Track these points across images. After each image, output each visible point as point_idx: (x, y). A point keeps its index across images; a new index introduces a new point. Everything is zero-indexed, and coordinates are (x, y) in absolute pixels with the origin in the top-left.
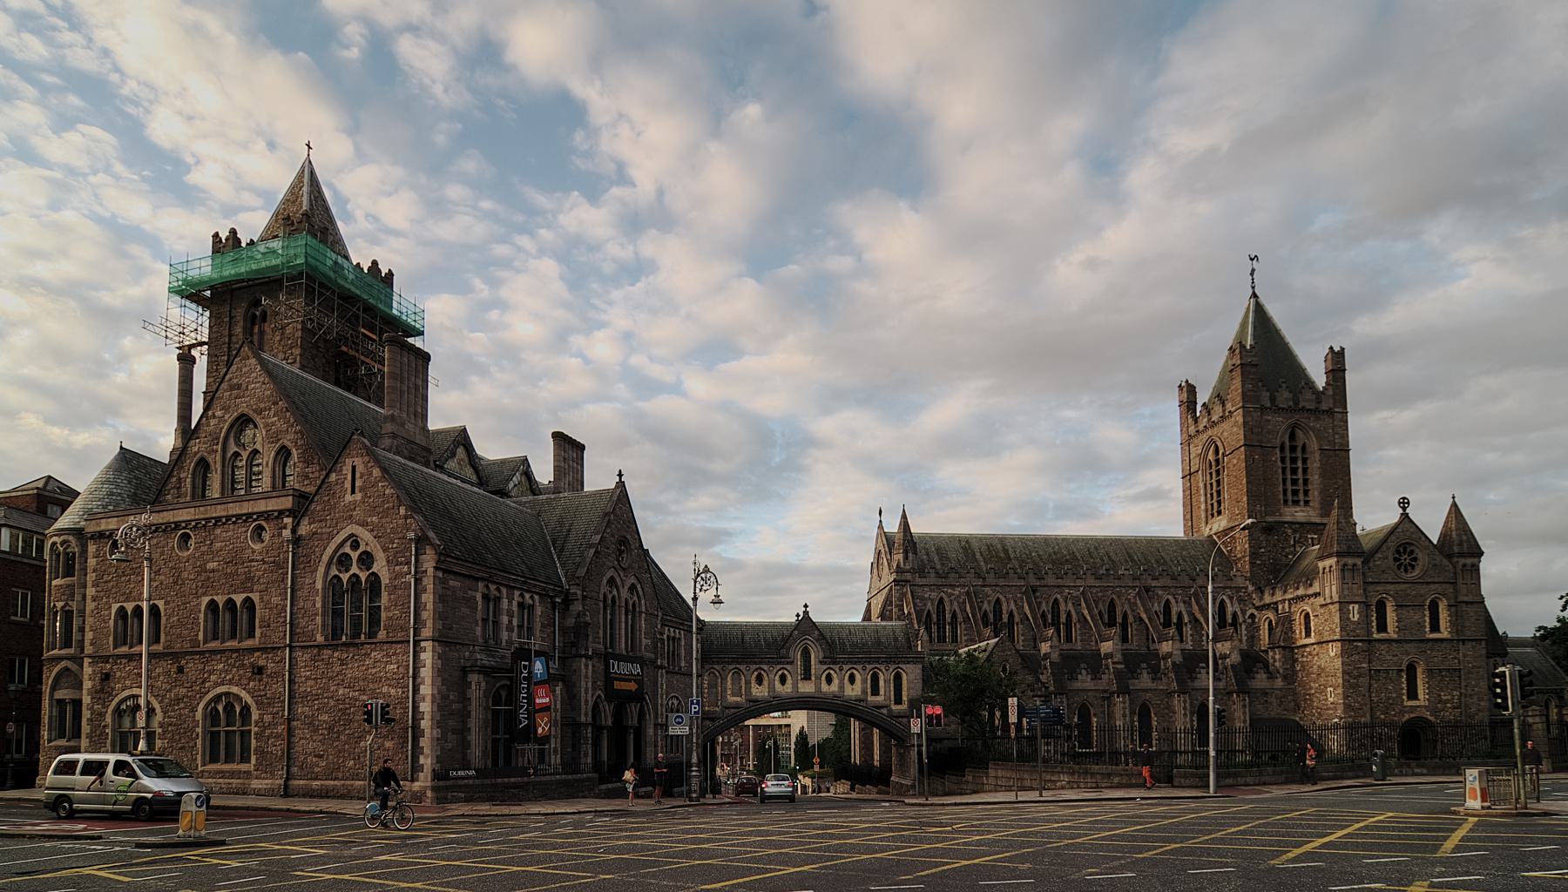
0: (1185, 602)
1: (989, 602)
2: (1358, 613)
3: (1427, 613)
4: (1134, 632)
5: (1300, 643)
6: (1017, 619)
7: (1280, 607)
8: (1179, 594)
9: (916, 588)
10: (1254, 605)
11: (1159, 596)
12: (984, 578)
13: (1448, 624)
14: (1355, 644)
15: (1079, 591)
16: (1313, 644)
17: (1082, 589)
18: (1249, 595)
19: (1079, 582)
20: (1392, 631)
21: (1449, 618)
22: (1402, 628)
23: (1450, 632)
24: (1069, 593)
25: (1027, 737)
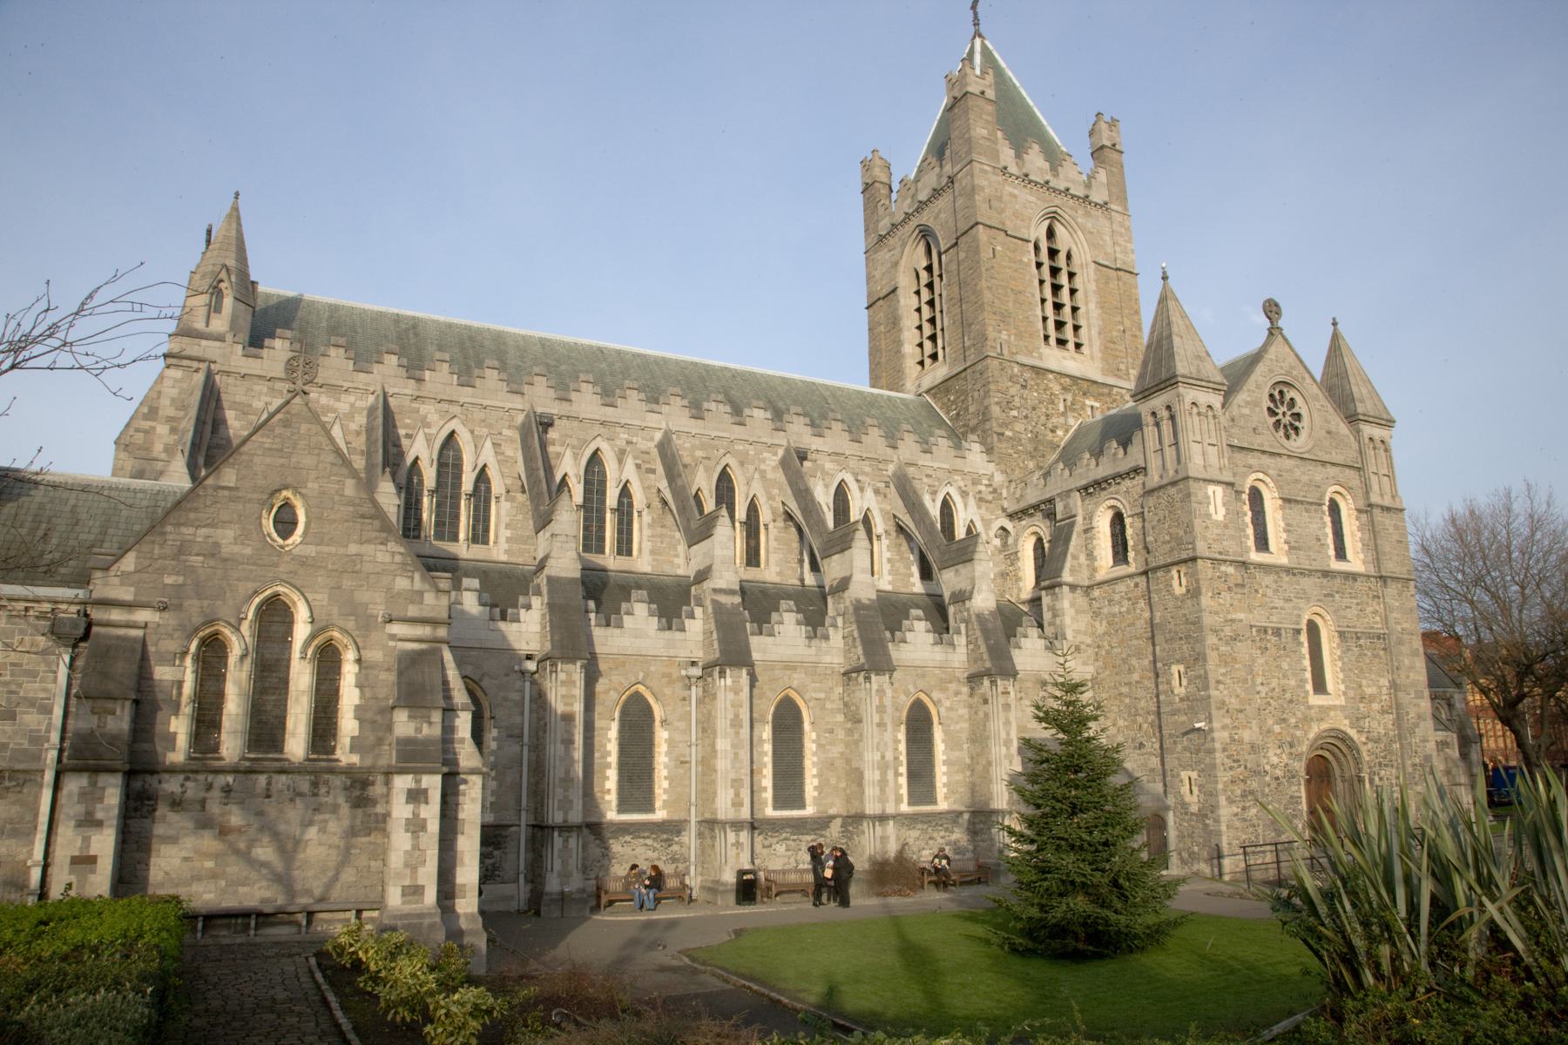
0: (877, 492)
1: (429, 440)
2: (1224, 504)
3: (1328, 519)
4: (773, 544)
5: (1102, 575)
6: (497, 487)
7: (1059, 507)
8: (867, 474)
9: (231, 380)
10: (1004, 510)
11: (825, 473)
12: (420, 380)
13: (1360, 545)
14: (1223, 568)
15: (652, 439)
16: (1131, 576)
17: (658, 436)
18: (995, 491)
19: (652, 420)
20: (1278, 553)
21: (1359, 534)
22: (1293, 544)
23: (1364, 562)
24: (629, 443)
25: (349, 771)
